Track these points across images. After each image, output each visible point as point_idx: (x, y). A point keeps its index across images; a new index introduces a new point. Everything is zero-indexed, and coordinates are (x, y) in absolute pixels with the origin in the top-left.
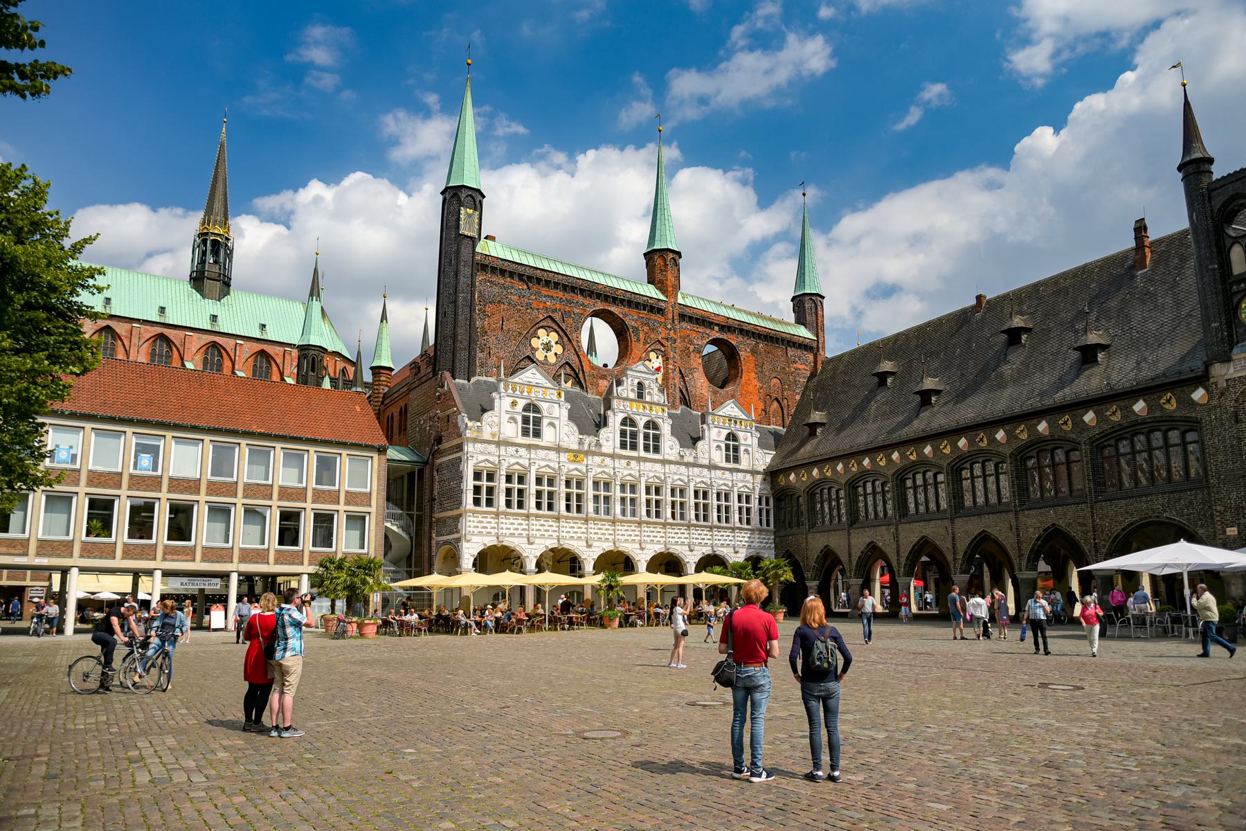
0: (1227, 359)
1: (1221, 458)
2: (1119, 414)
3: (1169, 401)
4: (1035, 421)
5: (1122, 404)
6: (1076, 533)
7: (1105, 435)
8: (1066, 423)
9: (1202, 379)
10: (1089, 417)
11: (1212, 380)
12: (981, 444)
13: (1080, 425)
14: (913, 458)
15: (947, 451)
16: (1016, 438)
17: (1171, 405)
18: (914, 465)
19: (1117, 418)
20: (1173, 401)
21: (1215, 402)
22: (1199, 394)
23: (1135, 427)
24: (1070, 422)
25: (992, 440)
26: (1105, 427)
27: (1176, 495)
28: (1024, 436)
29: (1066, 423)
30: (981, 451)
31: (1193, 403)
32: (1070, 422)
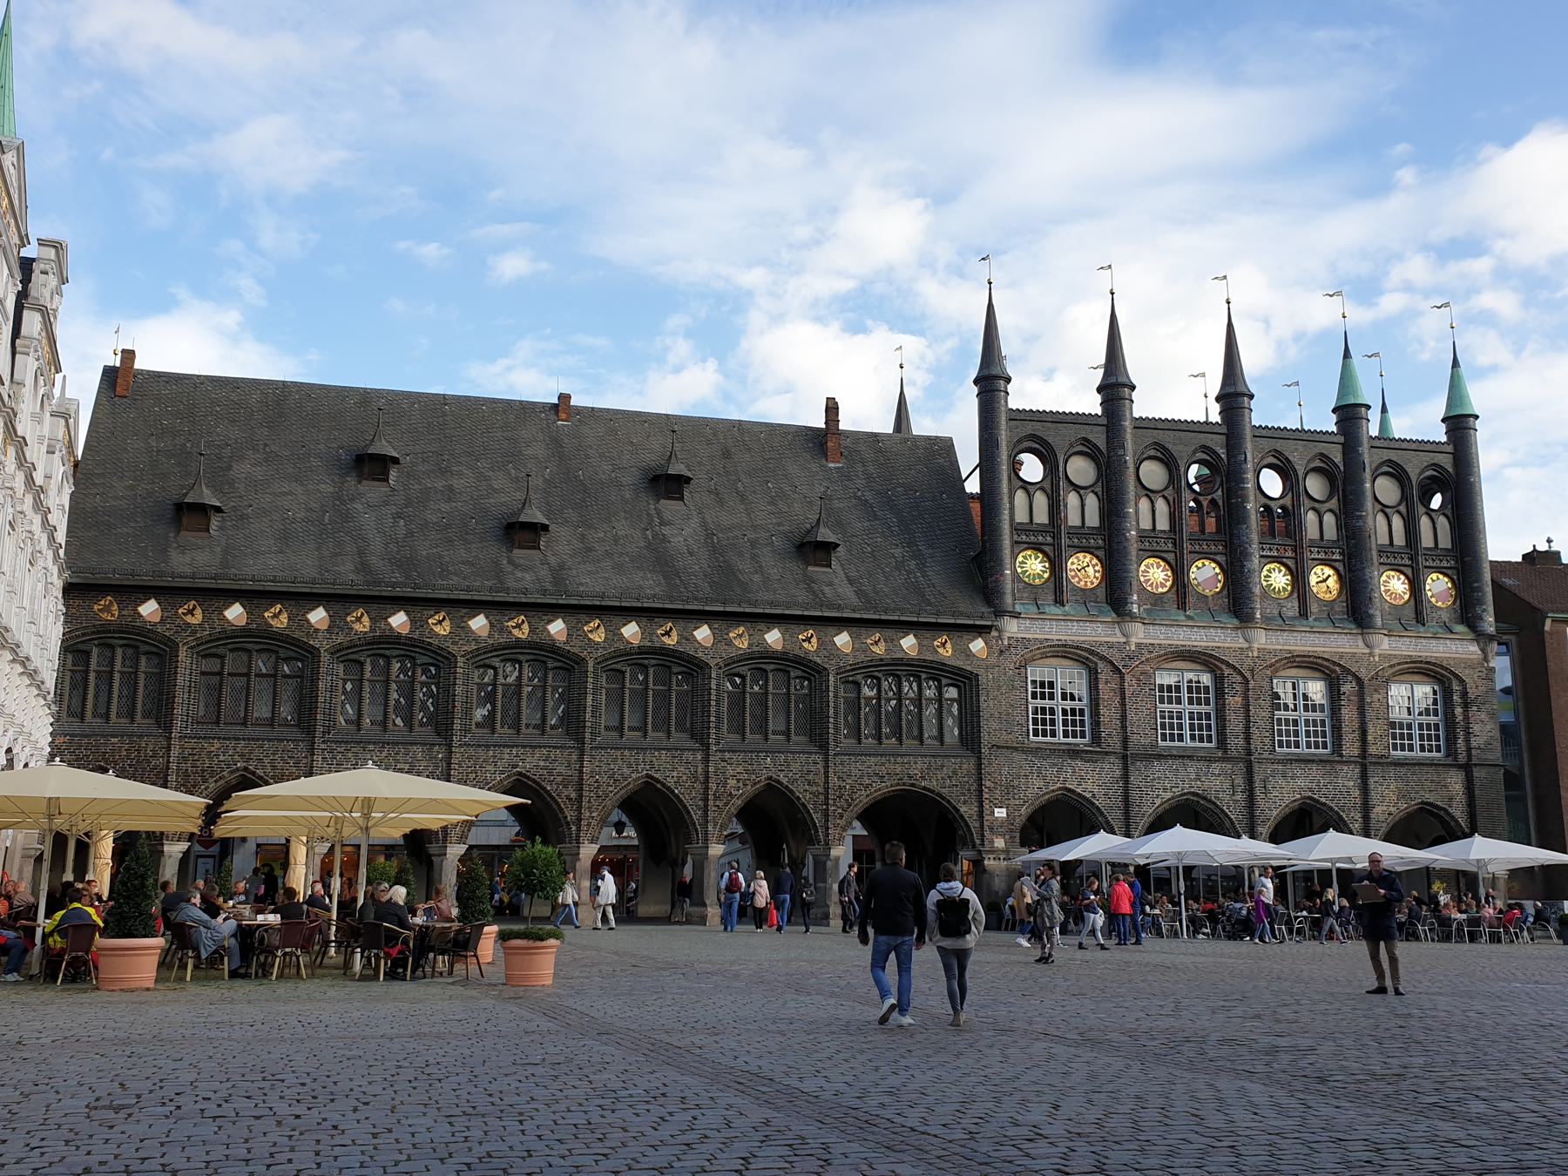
0: (1016, 616)
1: (994, 725)
2: (882, 645)
3: (943, 645)
4: (762, 626)
5: (889, 633)
6: (802, 792)
7: (855, 668)
8: (808, 640)
9: (981, 631)
10: (843, 640)
11: (994, 633)
12: (665, 639)
13: (827, 646)
14: (523, 633)
15: (599, 636)
16: (729, 643)
17: (945, 650)
18: (518, 644)
19: (880, 650)
20: (948, 645)
21: (993, 660)
22: (977, 646)
23: (900, 668)
24: (814, 640)
25: (688, 638)
26: (861, 658)
27: (939, 761)
28: (743, 645)
29: (809, 642)
30: (664, 652)
31: (969, 655)
32: (814, 640)
